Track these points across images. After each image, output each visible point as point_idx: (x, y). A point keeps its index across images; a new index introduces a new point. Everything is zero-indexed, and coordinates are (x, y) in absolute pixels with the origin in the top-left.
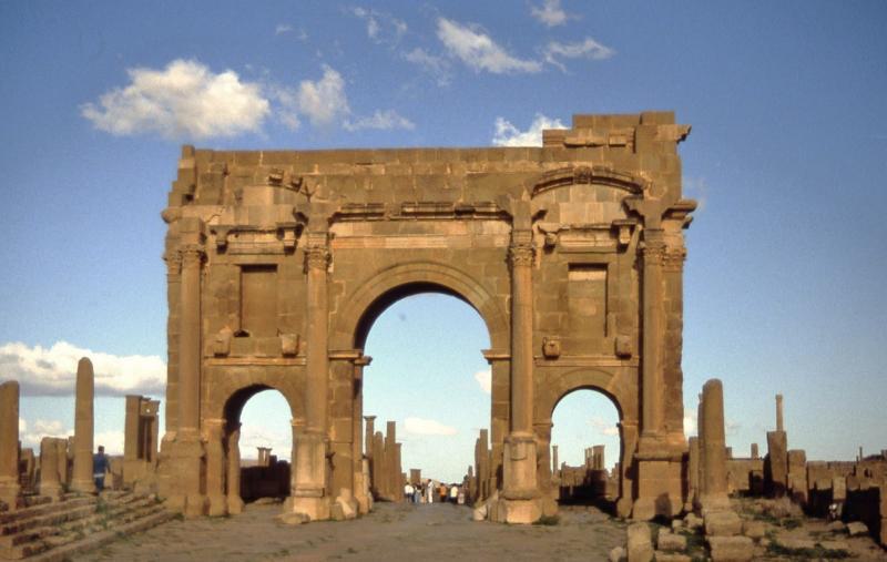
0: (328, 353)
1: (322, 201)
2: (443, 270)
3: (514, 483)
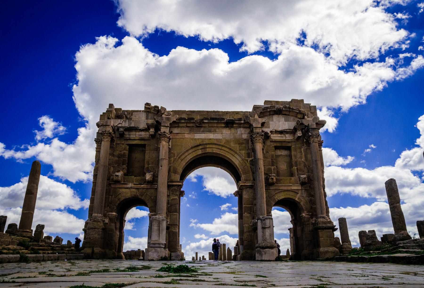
1: (168, 117)
2: (220, 147)
3: (264, 240)
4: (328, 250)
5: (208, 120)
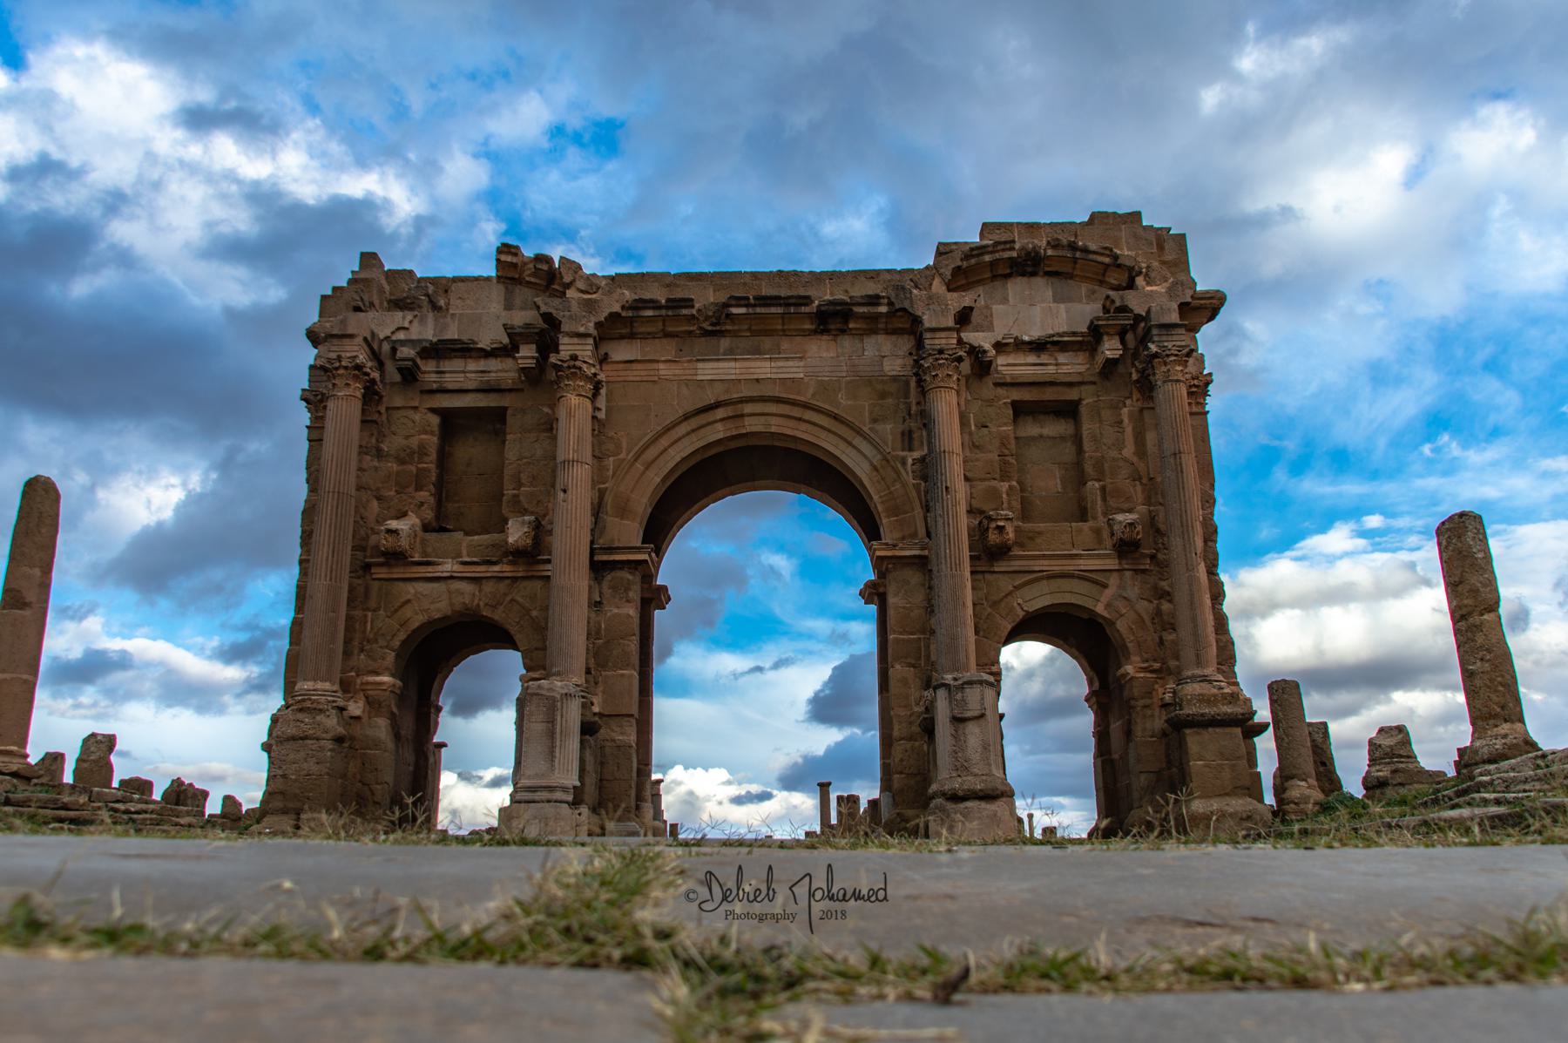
0: (592, 552)
1: (590, 296)
2: (797, 412)
3: (962, 768)
4: (1226, 808)
5: (746, 306)
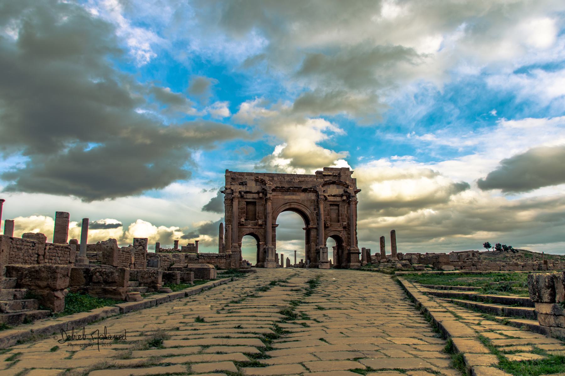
2: (299, 204)
3: (324, 259)
